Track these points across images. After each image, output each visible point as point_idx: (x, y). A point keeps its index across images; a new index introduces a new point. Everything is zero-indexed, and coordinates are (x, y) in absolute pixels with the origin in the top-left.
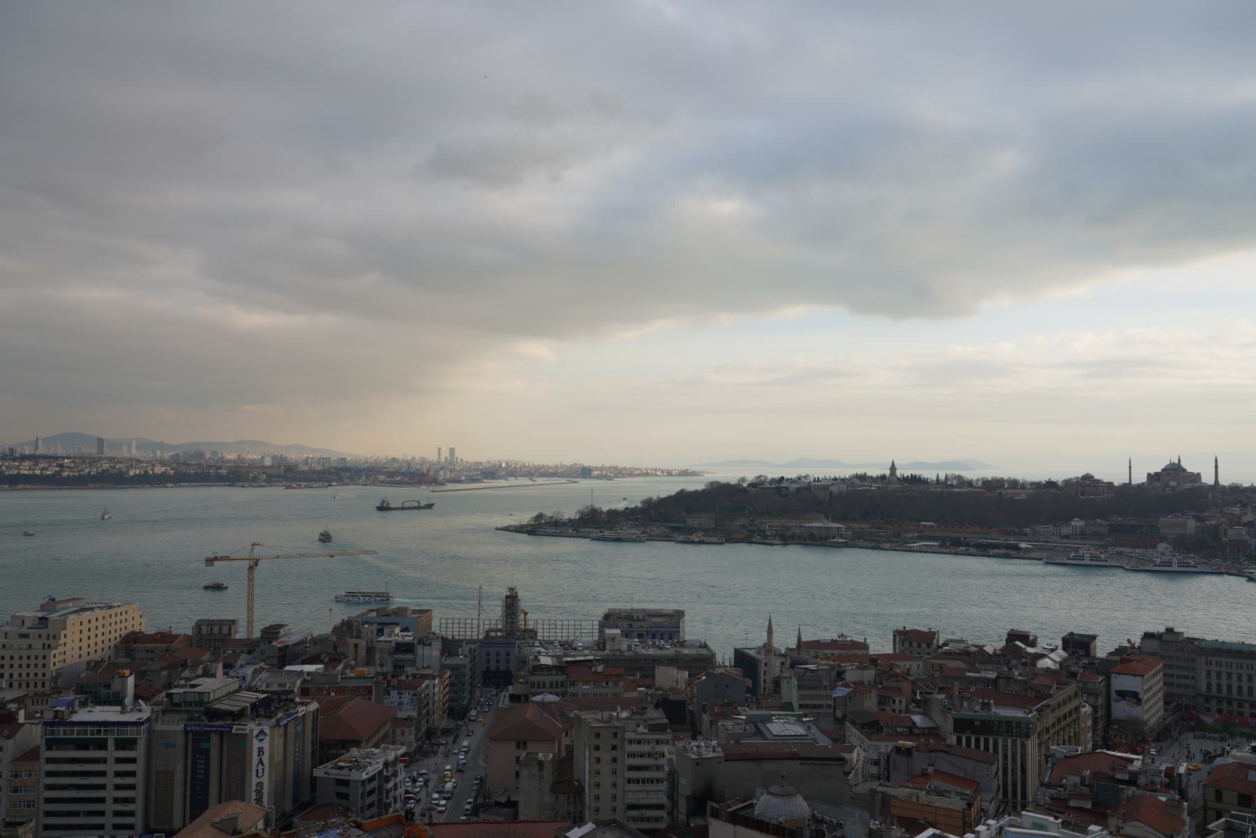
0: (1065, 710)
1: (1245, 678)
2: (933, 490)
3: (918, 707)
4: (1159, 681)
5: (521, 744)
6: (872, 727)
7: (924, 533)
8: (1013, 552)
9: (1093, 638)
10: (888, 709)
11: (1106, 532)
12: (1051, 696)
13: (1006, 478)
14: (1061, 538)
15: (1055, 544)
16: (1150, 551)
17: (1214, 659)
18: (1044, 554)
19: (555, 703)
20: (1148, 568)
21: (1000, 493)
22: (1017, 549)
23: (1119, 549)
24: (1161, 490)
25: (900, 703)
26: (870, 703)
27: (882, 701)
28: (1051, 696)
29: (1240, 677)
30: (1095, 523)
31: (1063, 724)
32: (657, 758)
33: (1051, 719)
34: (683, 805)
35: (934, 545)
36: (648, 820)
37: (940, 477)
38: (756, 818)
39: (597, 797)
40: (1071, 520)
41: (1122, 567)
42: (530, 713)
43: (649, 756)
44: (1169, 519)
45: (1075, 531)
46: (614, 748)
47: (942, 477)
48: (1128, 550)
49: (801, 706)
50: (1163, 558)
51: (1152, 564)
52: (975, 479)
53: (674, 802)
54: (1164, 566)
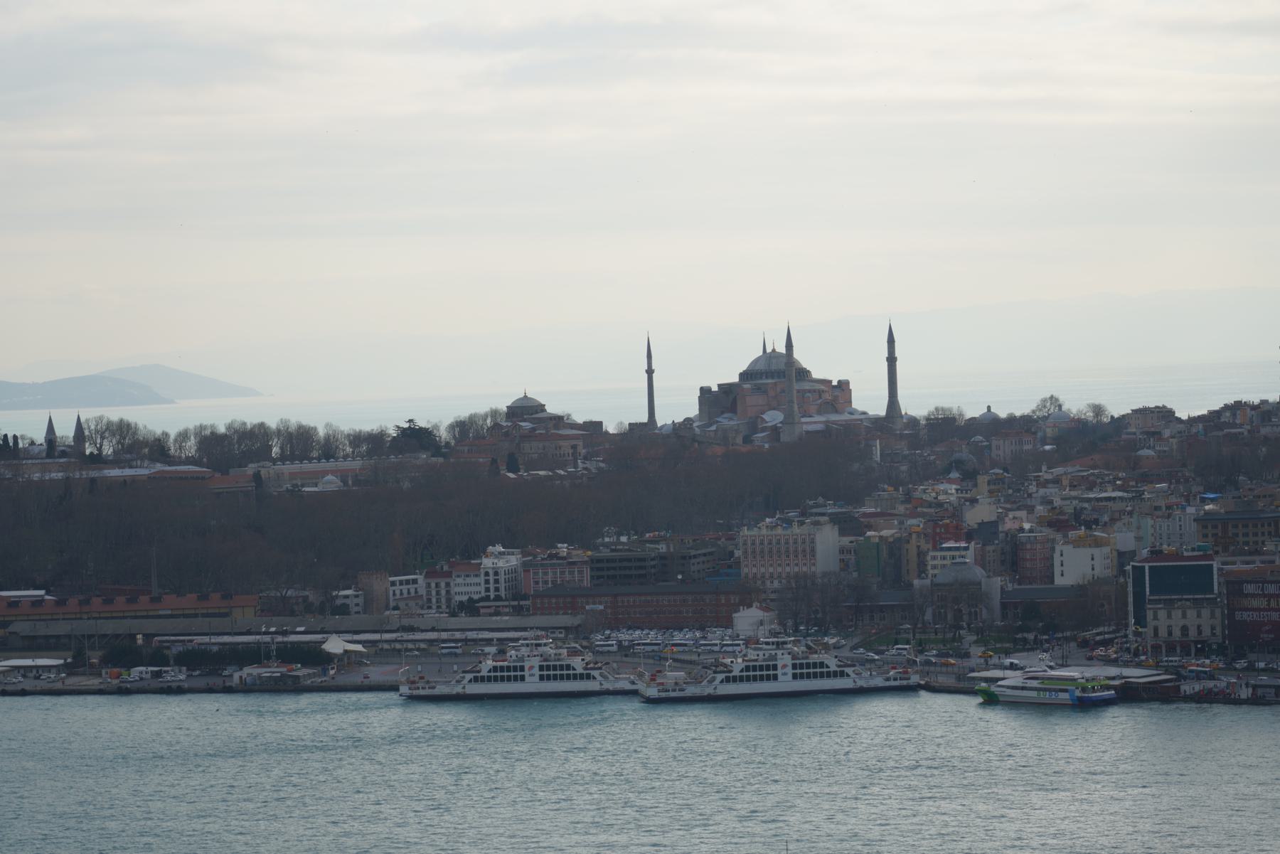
2: (36, 477)
7: (11, 628)
8: (305, 671)
11: (587, 582)
13: (272, 423)
14: (453, 614)
15: (432, 635)
16: (716, 636)
18: (398, 671)
20: (709, 691)
21: (257, 477)
22: (315, 657)
23: (625, 636)
24: (739, 440)
30: (551, 556)
35: (49, 668)
37: (59, 432)
40: (481, 551)
41: (634, 693)
44: (764, 530)
45: (492, 586)
47: (65, 431)
48: (653, 636)
50: (752, 654)
51: (720, 677)
52: (173, 434)
54: (755, 679)
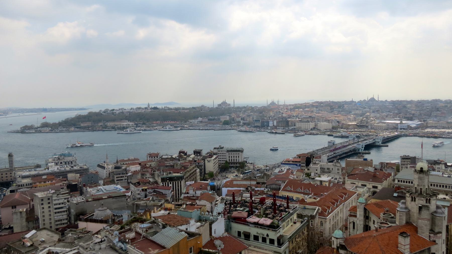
0: (192, 171)
1: (237, 157)
3: (152, 176)
4: (217, 160)
5: (14, 207)
6: (138, 184)
9: (202, 150)
10: (145, 178)
12: (188, 168)
17: (230, 153)
19: (28, 191)
25: (148, 175)
26: (139, 176)
27: (143, 175)
28: (188, 168)
29: (236, 157)
31: (192, 175)
32: (65, 204)
33: (188, 174)
34: (73, 218)
36: (63, 224)
38: (94, 219)
39: (44, 220)
42: (17, 196)
43: (62, 204)
46: (49, 203)
49: (117, 180)
53: (70, 218)
